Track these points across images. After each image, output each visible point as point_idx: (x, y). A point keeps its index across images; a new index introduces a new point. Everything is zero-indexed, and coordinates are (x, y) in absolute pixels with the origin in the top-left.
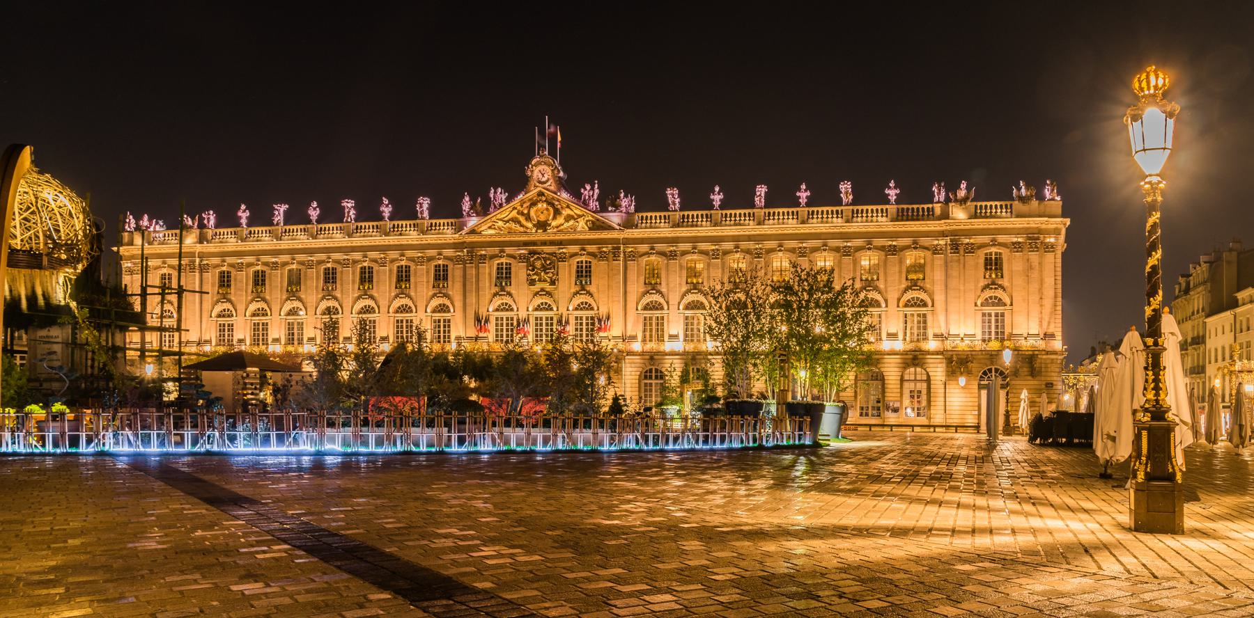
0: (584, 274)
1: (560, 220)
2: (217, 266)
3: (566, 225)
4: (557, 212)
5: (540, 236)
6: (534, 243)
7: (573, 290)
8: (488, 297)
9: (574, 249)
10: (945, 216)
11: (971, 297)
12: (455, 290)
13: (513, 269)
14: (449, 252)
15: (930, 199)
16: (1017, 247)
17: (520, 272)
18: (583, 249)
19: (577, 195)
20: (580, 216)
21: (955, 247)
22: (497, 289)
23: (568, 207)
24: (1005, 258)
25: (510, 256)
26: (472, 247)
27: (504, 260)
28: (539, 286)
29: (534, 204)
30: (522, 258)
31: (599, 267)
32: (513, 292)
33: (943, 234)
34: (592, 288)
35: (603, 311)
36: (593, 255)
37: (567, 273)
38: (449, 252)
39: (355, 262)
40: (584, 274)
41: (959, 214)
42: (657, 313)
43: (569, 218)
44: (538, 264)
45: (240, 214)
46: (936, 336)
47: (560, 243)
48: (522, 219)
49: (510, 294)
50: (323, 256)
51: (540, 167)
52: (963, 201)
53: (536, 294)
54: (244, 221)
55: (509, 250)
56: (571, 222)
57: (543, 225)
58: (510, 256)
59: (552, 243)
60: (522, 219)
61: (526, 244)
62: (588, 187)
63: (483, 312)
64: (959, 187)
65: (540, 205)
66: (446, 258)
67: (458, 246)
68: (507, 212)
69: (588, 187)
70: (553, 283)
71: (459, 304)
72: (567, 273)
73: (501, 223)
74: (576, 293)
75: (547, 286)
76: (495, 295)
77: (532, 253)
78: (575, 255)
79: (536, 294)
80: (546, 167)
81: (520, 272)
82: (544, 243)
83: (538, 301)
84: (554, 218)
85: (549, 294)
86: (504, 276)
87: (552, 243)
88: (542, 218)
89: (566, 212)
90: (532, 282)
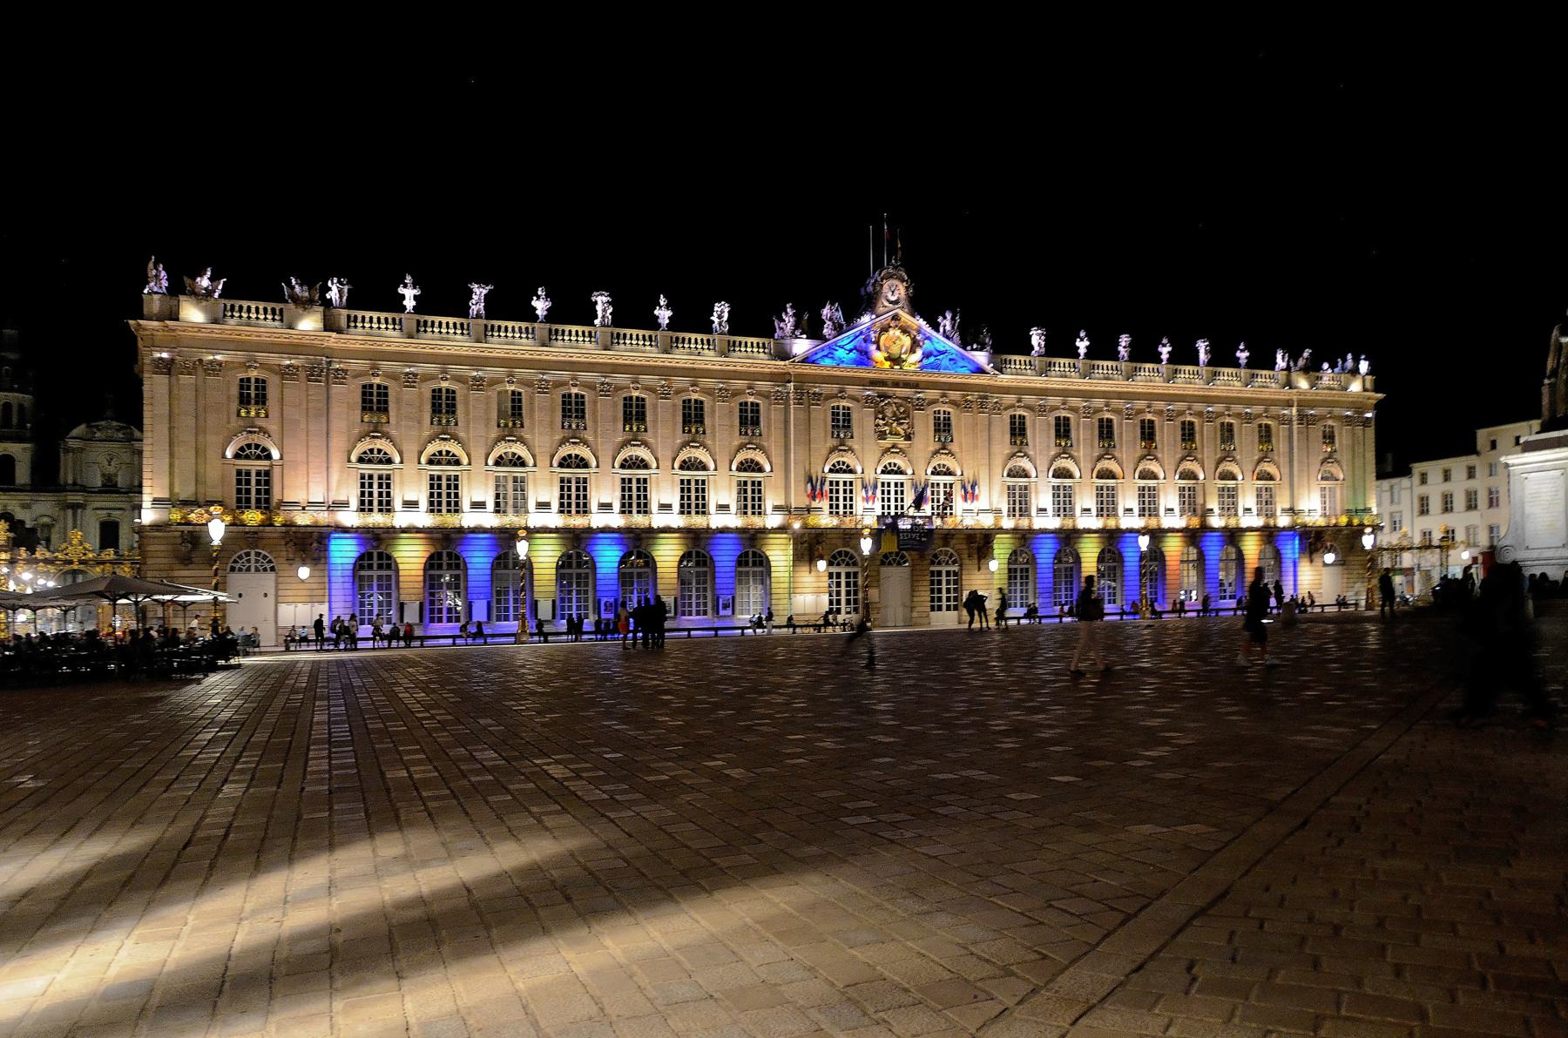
0: (943, 427)
1: (919, 354)
5: (896, 374)
6: (883, 383)
7: (932, 449)
8: (825, 452)
9: (932, 394)
12: (773, 441)
14: (763, 385)
17: (863, 420)
18: (944, 396)
19: (936, 327)
20: (942, 353)
22: (835, 442)
23: (929, 338)
24: (855, 416)
26: (801, 380)
27: (844, 403)
29: (885, 329)
31: (960, 421)
32: (855, 447)
34: (954, 447)
35: (969, 475)
36: (954, 403)
37: (923, 423)
38: (763, 385)
40: (943, 427)
44: (889, 414)
47: (915, 385)
49: (851, 449)
51: (891, 282)
53: (887, 451)
55: (852, 390)
56: (932, 359)
57: (896, 360)
59: (907, 385)
61: (874, 383)
63: (816, 471)
65: (891, 332)
70: (908, 437)
72: (923, 423)
74: (936, 452)
75: (902, 443)
76: (832, 451)
77: (883, 396)
78: (934, 402)
79: (887, 451)
80: (896, 282)
81: (863, 420)
82: (896, 384)
83: (887, 460)
84: (912, 351)
85: (902, 451)
86: (842, 423)
87: (907, 385)
88: (895, 350)
90: (882, 435)
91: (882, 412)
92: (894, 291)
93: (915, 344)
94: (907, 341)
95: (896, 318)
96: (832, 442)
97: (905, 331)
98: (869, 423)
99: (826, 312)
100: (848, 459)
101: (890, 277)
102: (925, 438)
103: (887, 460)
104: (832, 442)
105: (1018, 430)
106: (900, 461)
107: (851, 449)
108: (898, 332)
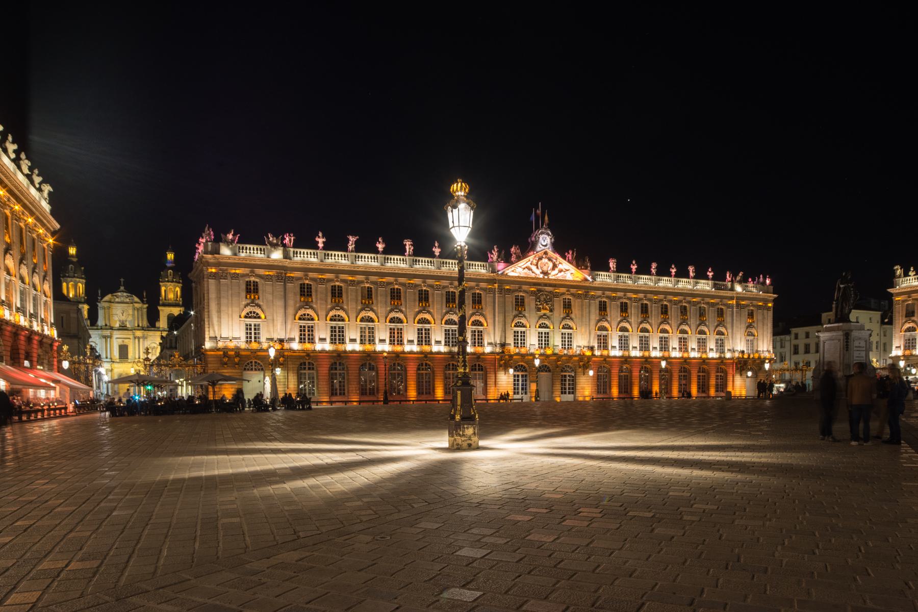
0: (567, 306)
1: (556, 271)
2: (300, 279)
3: (560, 274)
4: (555, 266)
8: (512, 317)
9: (563, 290)
10: (732, 289)
11: (743, 330)
12: (488, 312)
13: (526, 300)
14: (483, 285)
15: (724, 279)
16: (759, 307)
17: (530, 302)
21: (738, 305)
25: (525, 291)
26: (502, 282)
28: (543, 312)
29: (540, 259)
30: (532, 293)
31: (576, 304)
33: (732, 298)
34: (573, 316)
38: (483, 285)
39: (416, 286)
40: (567, 306)
41: (738, 288)
42: (604, 333)
43: (561, 271)
44: (542, 298)
45: (317, 239)
46: (729, 350)
47: (554, 286)
48: (534, 268)
49: (524, 316)
50: (391, 279)
52: (740, 282)
53: (541, 317)
54: (321, 245)
55: (525, 287)
57: (545, 273)
58: (525, 291)
60: (534, 268)
62: (571, 252)
64: (738, 274)
66: (482, 289)
67: (492, 281)
68: (523, 263)
69: (571, 252)
70: (551, 311)
71: (490, 321)
73: (520, 270)
76: (515, 317)
77: (539, 291)
78: (563, 294)
81: (530, 302)
82: (546, 285)
83: (541, 321)
84: (553, 269)
85: (548, 318)
87: (550, 285)
88: (545, 269)
89: (560, 267)
90: (539, 310)
91: (539, 298)
92: (545, 240)
93: (555, 266)
94: (551, 265)
95: (546, 253)
96: (515, 313)
97: (550, 260)
98: (533, 305)
99: (513, 250)
100: (523, 321)
101: (542, 233)
102: (559, 312)
103: (541, 321)
104: (515, 313)
105: (603, 308)
106: (547, 322)
107: (524, 316)
108: (546, 260)
